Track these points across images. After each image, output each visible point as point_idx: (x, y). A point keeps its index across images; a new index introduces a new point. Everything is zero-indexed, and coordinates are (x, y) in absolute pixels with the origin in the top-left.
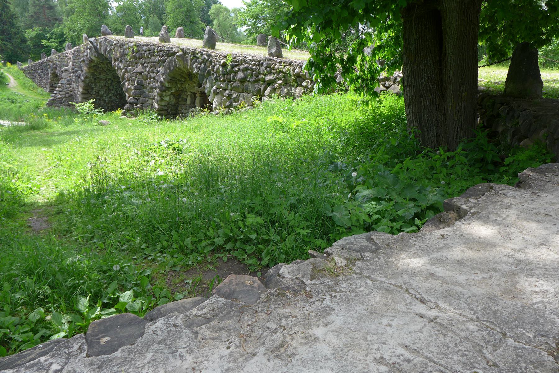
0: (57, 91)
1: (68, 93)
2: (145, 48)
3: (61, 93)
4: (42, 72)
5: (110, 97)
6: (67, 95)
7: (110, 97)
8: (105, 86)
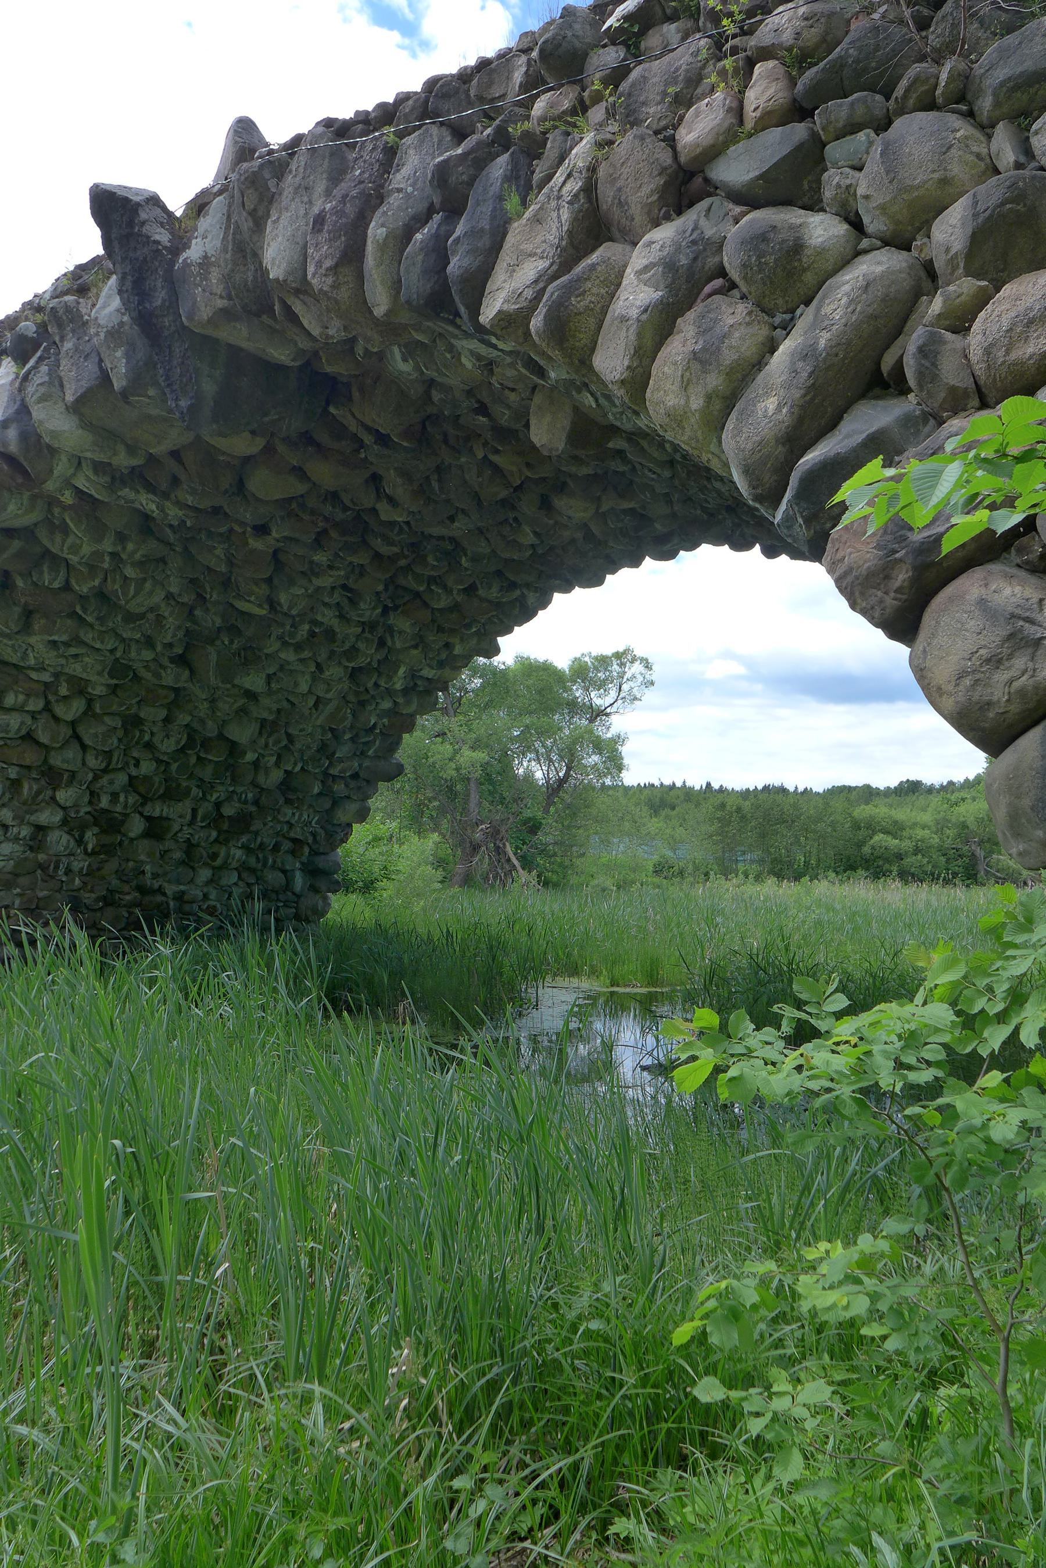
7: (40, 828)
8: (29, 737)
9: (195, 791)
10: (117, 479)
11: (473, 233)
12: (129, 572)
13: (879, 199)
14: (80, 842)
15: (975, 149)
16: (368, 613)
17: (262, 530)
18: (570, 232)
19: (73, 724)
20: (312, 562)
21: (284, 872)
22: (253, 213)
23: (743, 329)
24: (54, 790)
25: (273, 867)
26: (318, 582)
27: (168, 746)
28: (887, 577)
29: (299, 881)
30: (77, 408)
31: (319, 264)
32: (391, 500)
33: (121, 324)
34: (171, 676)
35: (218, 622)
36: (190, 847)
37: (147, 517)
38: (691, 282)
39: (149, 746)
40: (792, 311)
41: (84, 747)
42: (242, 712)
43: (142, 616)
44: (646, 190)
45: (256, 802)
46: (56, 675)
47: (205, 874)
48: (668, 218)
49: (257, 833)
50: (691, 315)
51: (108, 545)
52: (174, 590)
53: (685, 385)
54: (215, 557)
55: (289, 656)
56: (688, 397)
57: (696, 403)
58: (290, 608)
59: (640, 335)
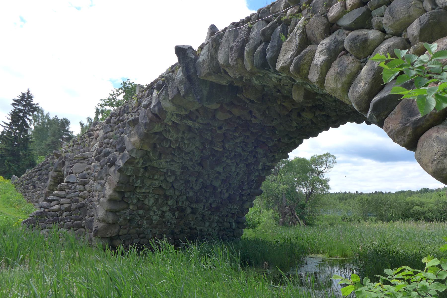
0: (55, 195)
1: (77, 201)
3: (62, 201)
4: (39, 179)
6: (74, 206)
7: (163, 212)
8: (161, 187)
9: (204, 200)
10: (183, 118)
11: (273, 47)
12: (186, 141)
13: (390, 24)
14: (174, 215)
15: (418, 6)
16: (250, 149)
17: (220, 128)
18: (299, 43)
19: (172, 183)
20: (234, 136)
21: (230, 223)
22: (215, 48)
23: (352, 64)
26: (236, 141)
27: (197, 188)
28: (404, 132)
29: (234, 225)
30: (172, 101)
31: (232, 59)
32: (255, 117)
33: (183, 79)
34: (197, 169)
35: (209, 153)
36: (203, 216)
37: (190, 127)
38: (334, 53)
39: (192, 188)
40: (366, 57)
41: (174, 189)
42: (217, 178)
43: (189, 153)
44: (320, 30)
45: (221, 203)
46: (167, 170)
47: (208, 224)
48: (327, 36)
50: (336, 62)
51: (180, 135)
52: (198, 145)
53: (336, 81)
54: (208, 136)
55: (229, 161)
56: (337, 84)
57: (340, 86)
58: (229, 148)
59: (321, 69)
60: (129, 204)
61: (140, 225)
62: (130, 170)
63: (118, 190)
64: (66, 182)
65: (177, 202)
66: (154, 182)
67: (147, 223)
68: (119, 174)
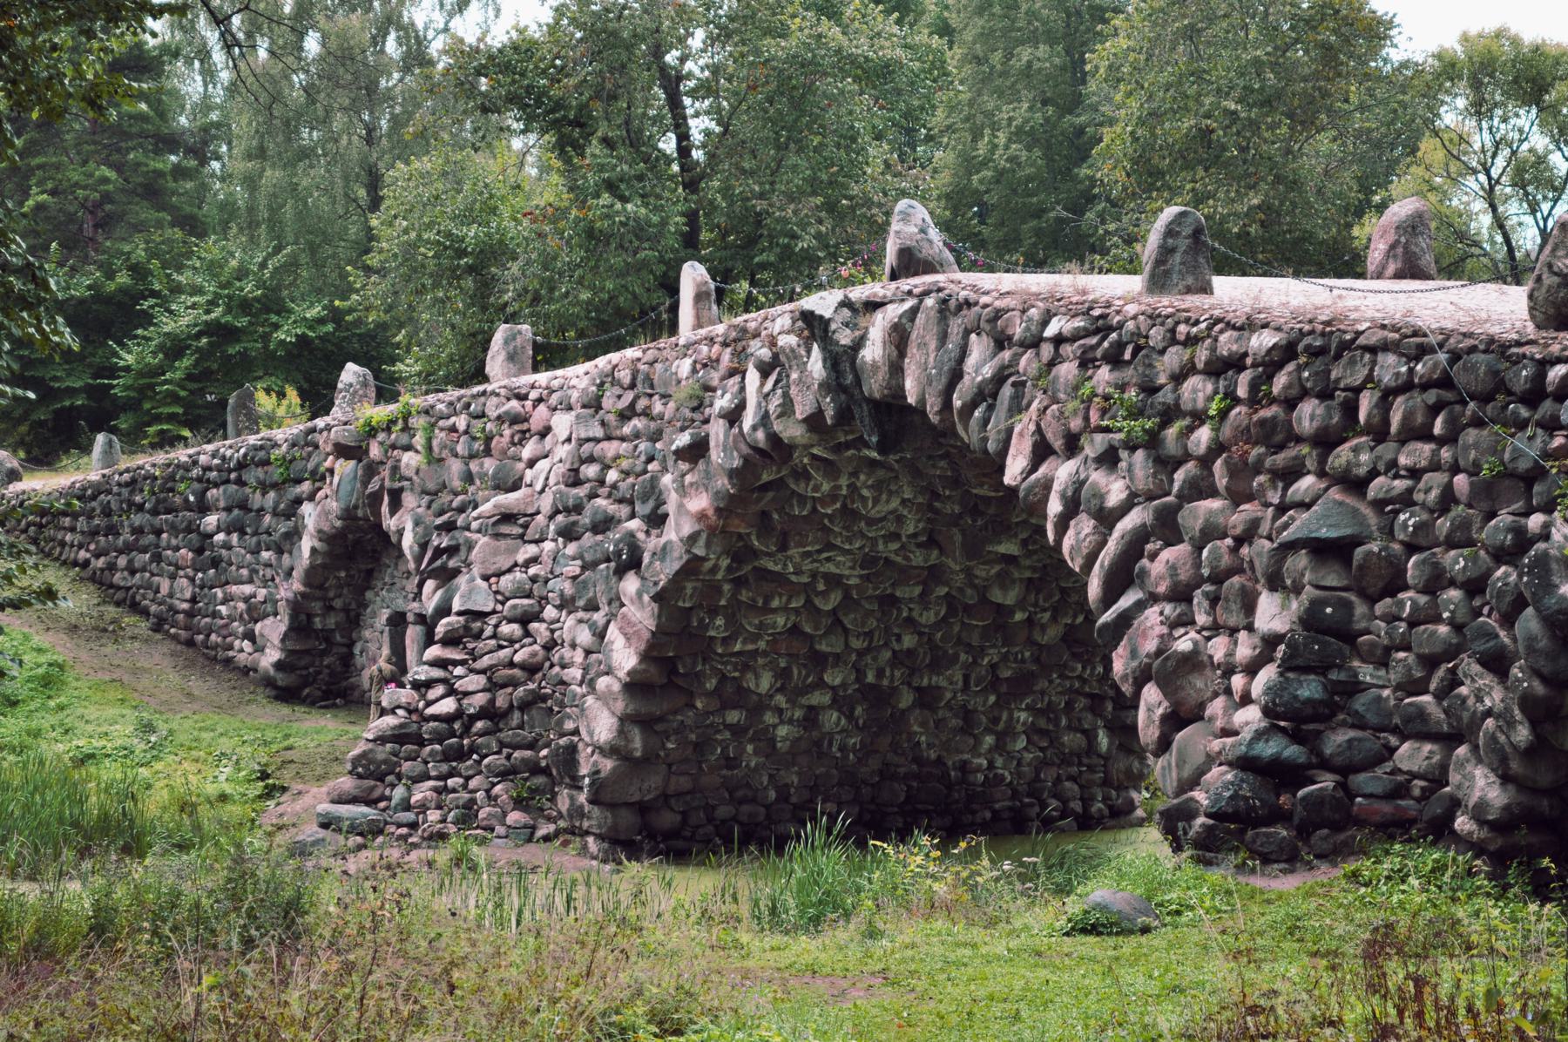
2: (1390, 367)
5: (811, 717)
7: (812, 710)
8: (795, 630)
9: (963, 657)
12: (865, 492)
19: (834, 611)
21: (1084, 732)
24: (823, 670)
25: (1070, 728)
27: (928, 618)
29: (1103, 740)
34: (917, 558)
36: (967, 715)
39: (910, 621)
41: (846, 631)
47: (989, 740)
49: (1043, 693)
60: (691, 695)
61: (735, 758)
62: (689, 591)
63: (655, 654)
64: (460, 614)
65: (858, 671)
66: (769, 619)
67: (756, 753)
68: (655, 606)
